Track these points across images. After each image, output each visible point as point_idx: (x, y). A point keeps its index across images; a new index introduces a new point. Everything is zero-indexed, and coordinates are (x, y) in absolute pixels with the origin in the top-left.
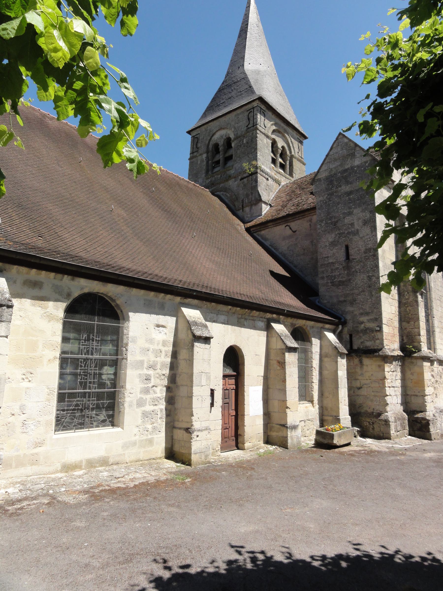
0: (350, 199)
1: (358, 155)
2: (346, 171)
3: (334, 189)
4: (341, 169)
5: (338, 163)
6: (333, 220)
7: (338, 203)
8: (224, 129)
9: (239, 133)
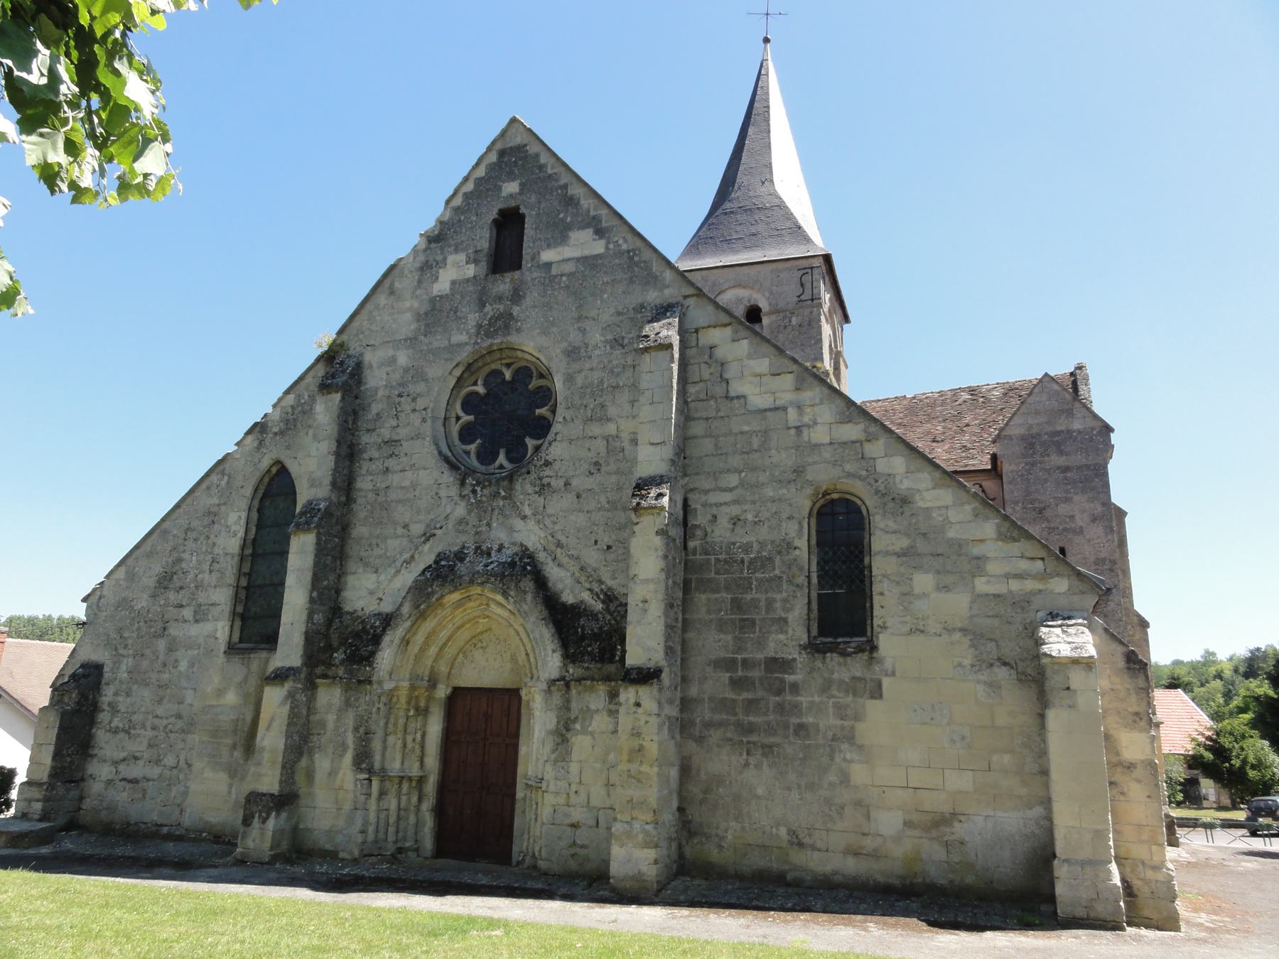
0: (1066, 478)
1: (1079, 415)
2: (1058, 433)
3: (1037, 457)
4: (1049, 429)
5: (1042, 419)
6: (1037, 505)
7: (1046, 481)
8: (744, 287)
9: (781, 305)
